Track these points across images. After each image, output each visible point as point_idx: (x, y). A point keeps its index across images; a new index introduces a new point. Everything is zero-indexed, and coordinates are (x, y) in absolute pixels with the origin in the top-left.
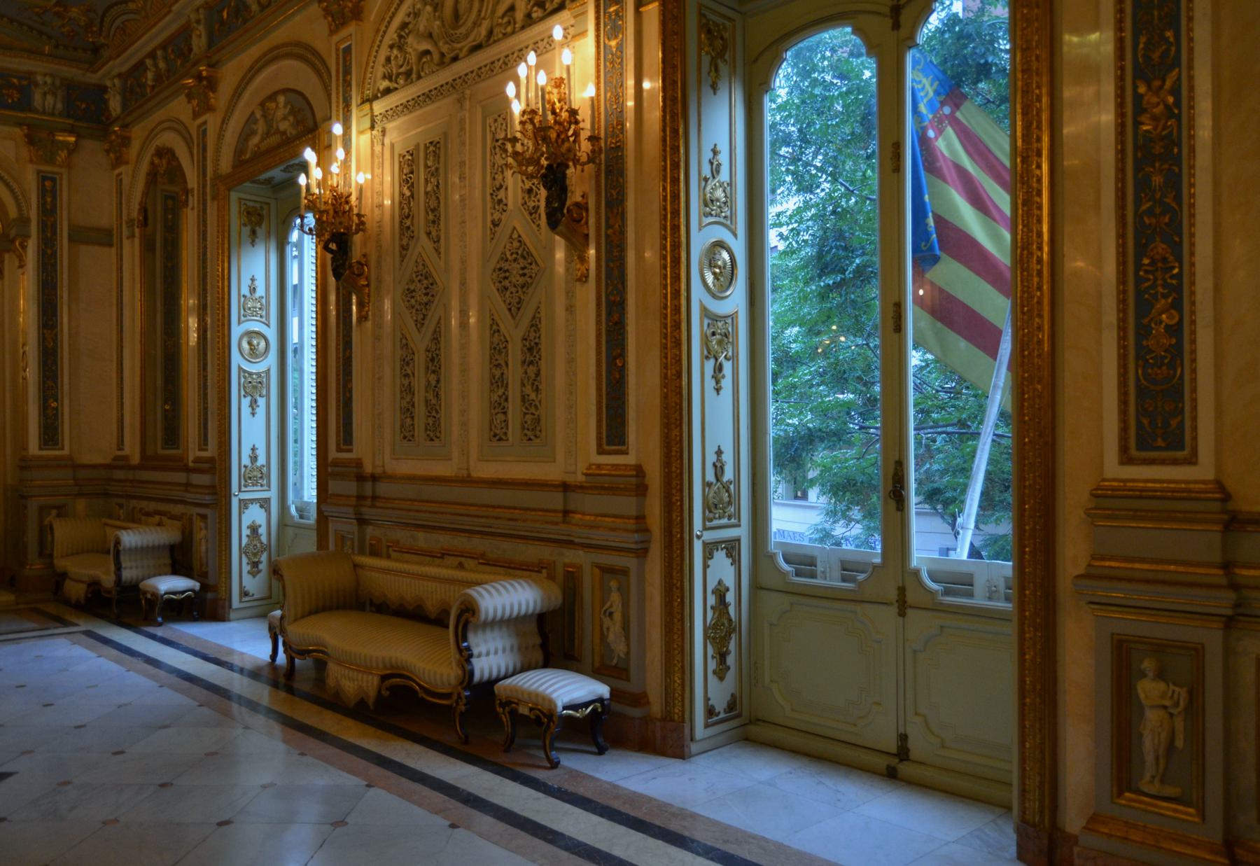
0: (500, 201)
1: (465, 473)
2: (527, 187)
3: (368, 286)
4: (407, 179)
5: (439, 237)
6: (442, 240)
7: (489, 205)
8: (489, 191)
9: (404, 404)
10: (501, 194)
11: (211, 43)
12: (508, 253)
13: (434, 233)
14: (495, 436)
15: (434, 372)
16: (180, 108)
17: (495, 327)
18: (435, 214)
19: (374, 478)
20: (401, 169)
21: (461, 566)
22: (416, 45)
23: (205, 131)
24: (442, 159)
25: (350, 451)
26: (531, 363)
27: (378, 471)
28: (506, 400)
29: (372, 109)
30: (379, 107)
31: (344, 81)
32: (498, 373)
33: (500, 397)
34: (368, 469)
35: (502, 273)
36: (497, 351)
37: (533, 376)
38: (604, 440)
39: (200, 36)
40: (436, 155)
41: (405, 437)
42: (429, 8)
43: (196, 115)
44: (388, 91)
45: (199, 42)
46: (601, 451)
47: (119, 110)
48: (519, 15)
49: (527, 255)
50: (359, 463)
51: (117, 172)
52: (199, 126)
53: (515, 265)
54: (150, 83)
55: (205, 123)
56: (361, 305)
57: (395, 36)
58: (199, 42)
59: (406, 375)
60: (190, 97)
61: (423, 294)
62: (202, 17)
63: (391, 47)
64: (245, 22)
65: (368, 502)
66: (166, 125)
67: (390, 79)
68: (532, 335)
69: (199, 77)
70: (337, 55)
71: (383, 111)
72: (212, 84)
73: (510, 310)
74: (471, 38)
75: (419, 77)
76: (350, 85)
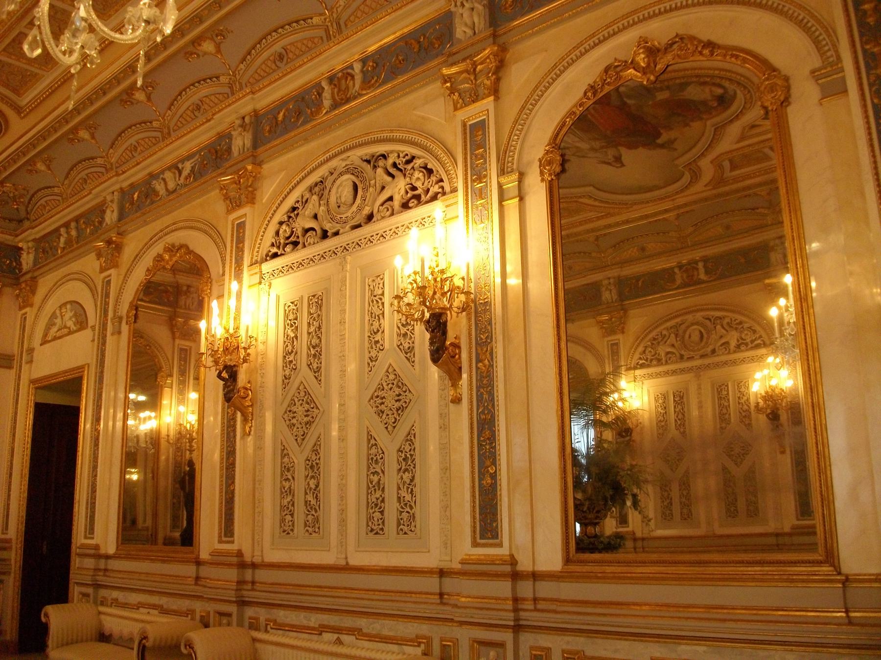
0: (377, 342)
1: (343, 563)
2: (402, 332)
3: (252, 406)
4: (292, 321)
5: (319, 369)
6: (323, 369)
7: (367, 345)
8: (367, 334)
9: (285, 502)
10: (378, 337)
11: (121, 217)
12: (385, 384)
13: (315, 366)
14: (372, 530)
15: (313, 477)
16: (89, 264)
17: (373, 442)
18: (316, 351)
19: (254, 566)
20: (286, 316)
21: (339, 642)
22: (303, 222)
23: (109, 282)
24: (324, 308)
25: (233, 542)
26: (406, 470)
27: (257, 560)
28: (383, 501)
29: (260, 269)
30: (267, 267)
31: (237, 247)
32: (375, 479)
33: (377, 499)
34: (248, 558)
35: (377, 399)
36: (374, 460)
37: (408, 481)
38: (478, 536)
39: (113, 211)
40: (320, 306)
41: (284, 531)
42: (315, 197)
43: (102, 270)
44: (275, 255)
45: (111, 217)
46: (475, 544)
47: (31, 262)
48: (397, 203)
49: (401, 385)
50: (240, 554)
51: (24, 311)
52: (106, 278)
53: (391, 393)
54: (62, 245)
55: (110, 276)
56: (245, 420)
57: (285, 216)
58: (111, 217)
59: (287, 480)
60: (99, 256)
61: (303, 412)
62: (116, 198)
63: (281, 223)
64: (152, 202)
65: (249, 587)
66: (76, 276)
67: (279, 248)
68: (407, 448)
69: (109, 242)
70: (233, 228)
71: (270, 270)
72: (119, 248)
73: (387, 428)
74: (355, 219)
75: (304, 246)
76: (242, 251)
